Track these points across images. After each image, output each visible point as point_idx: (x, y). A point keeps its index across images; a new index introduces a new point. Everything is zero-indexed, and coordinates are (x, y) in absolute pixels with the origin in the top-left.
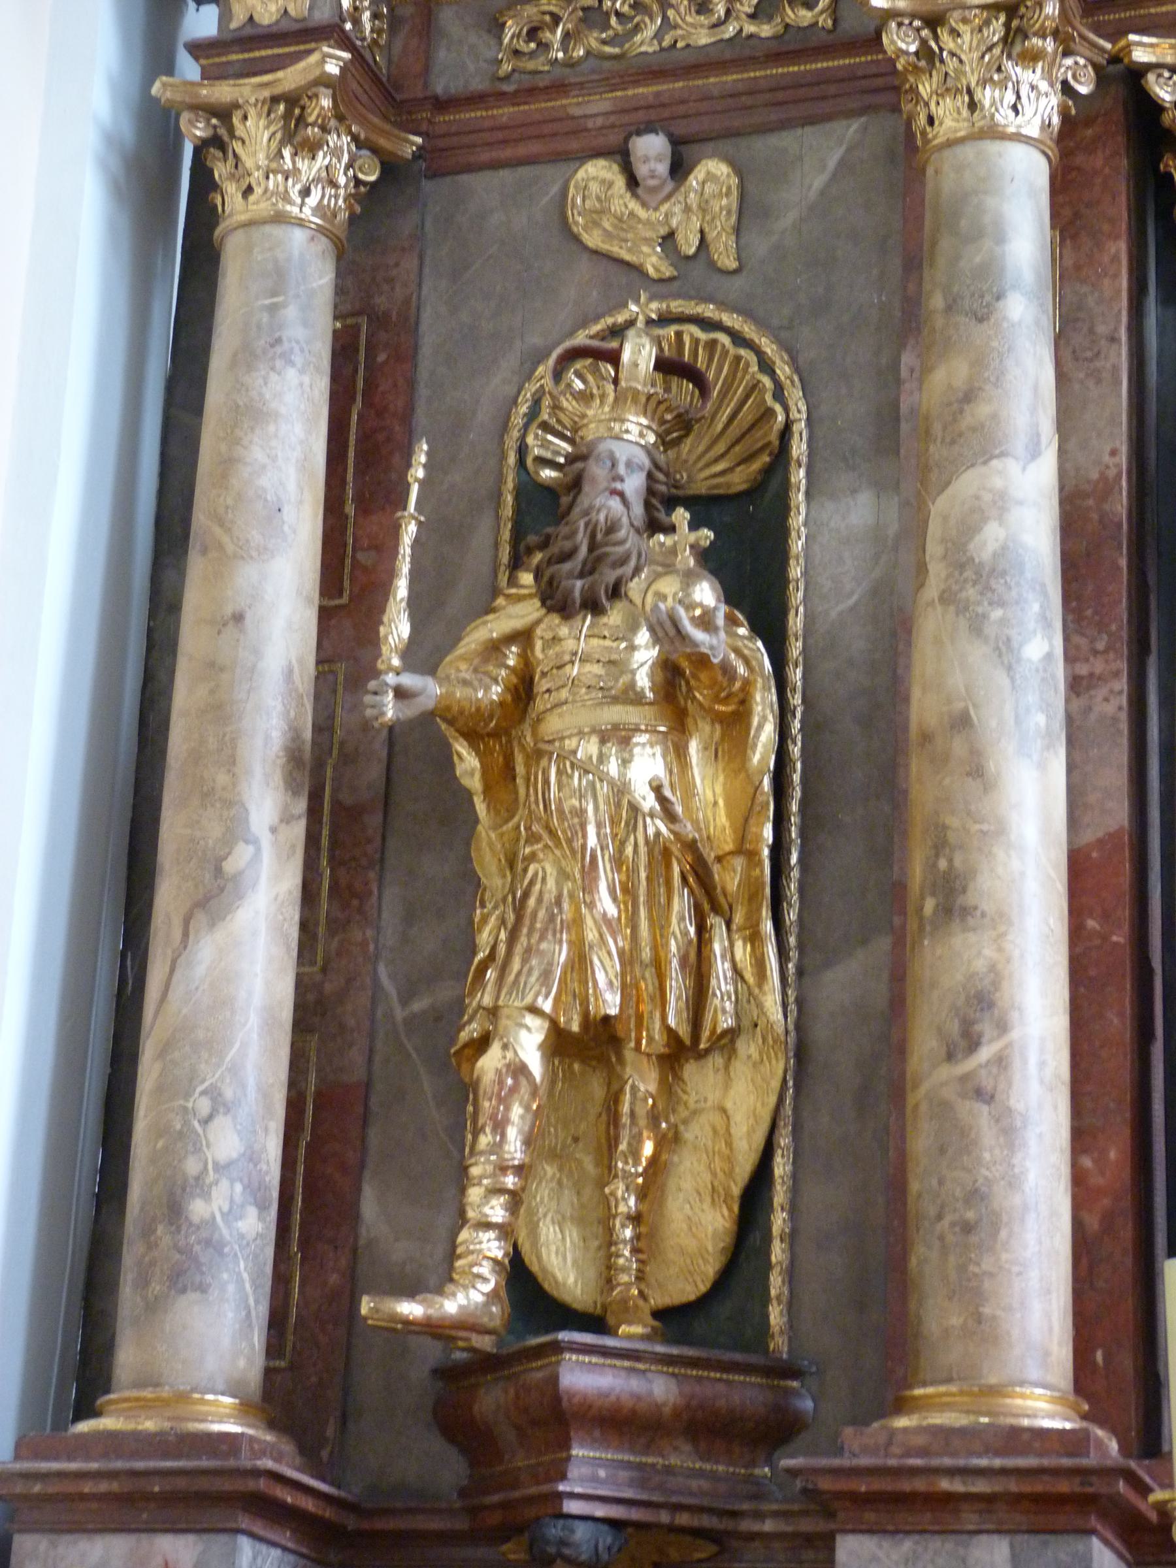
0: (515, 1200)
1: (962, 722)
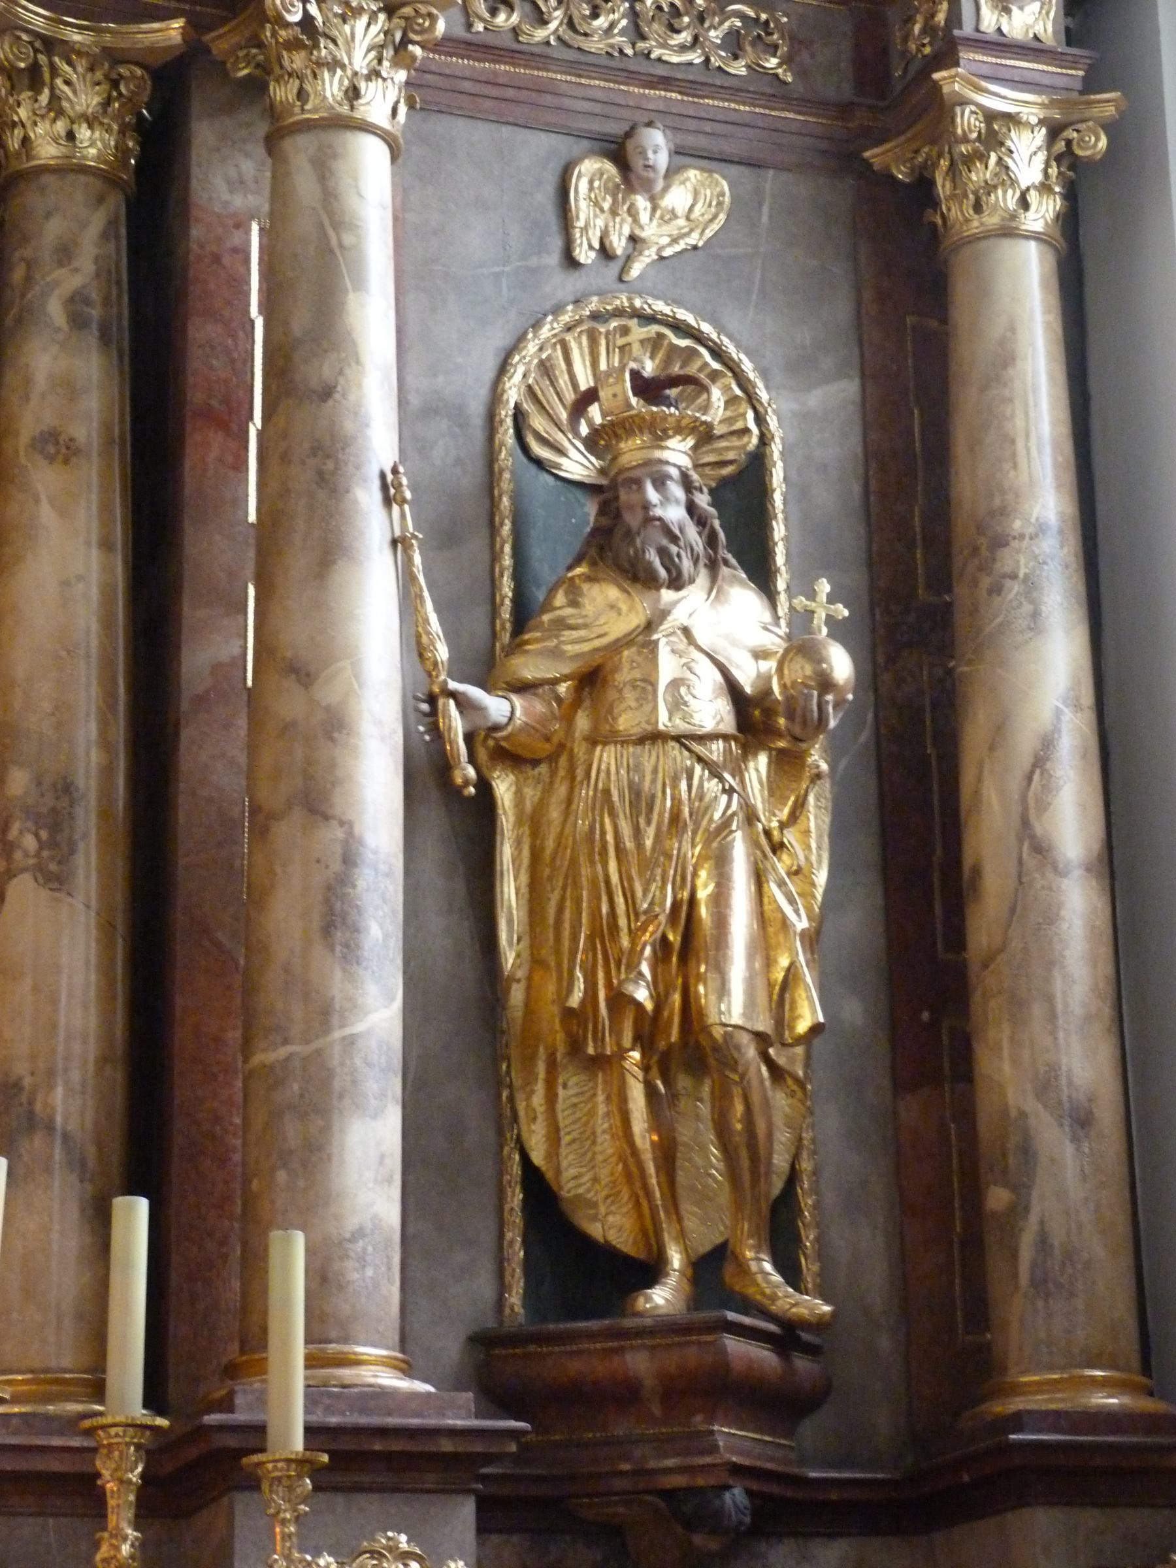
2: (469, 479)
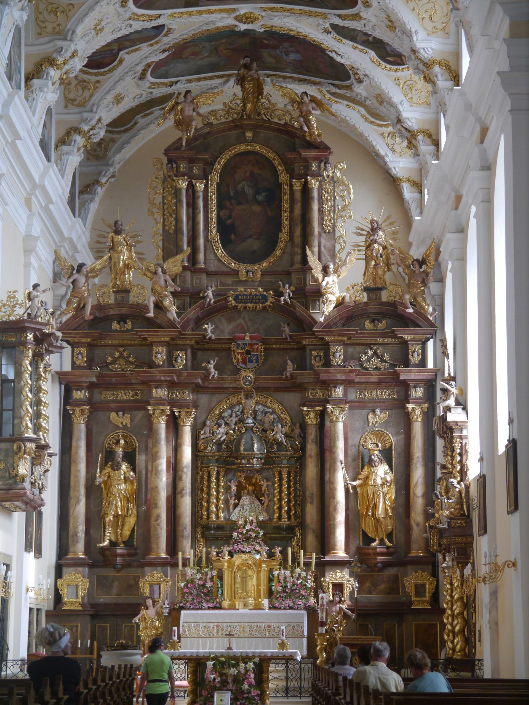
0: (110, 533)
1: (157, 487)
2: (356, 453)
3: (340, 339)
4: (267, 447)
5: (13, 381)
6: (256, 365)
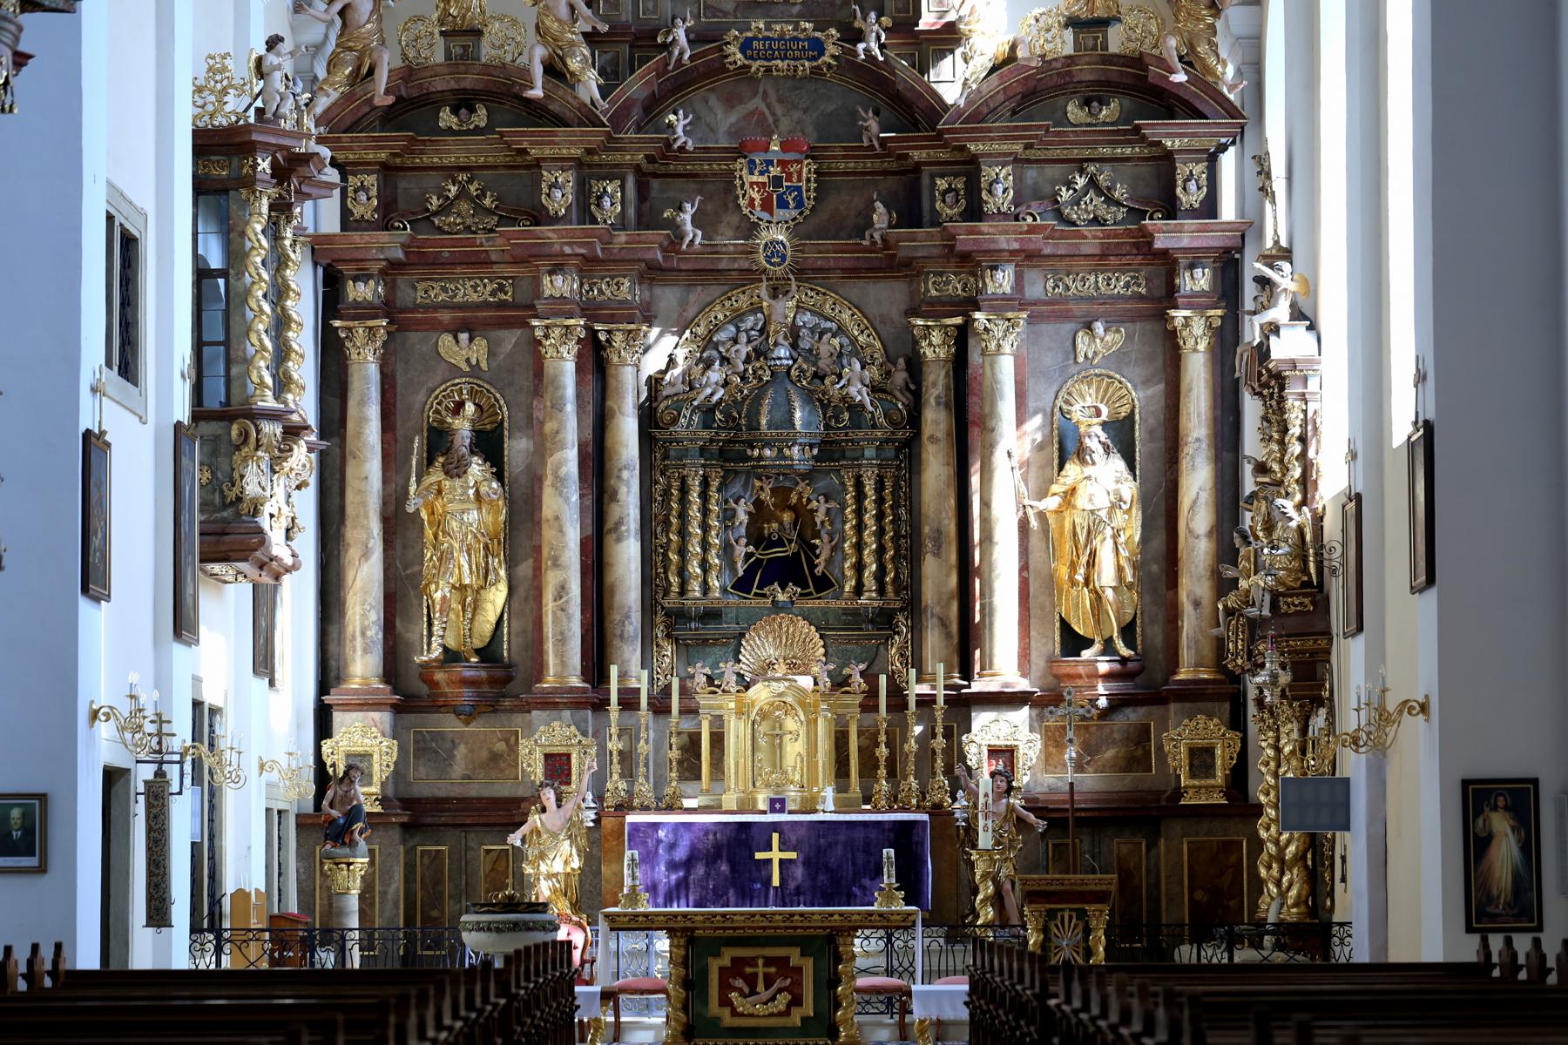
3: (1005, 148)
4: (824, 414)
5: (223, 273)
6: (794, 213)
